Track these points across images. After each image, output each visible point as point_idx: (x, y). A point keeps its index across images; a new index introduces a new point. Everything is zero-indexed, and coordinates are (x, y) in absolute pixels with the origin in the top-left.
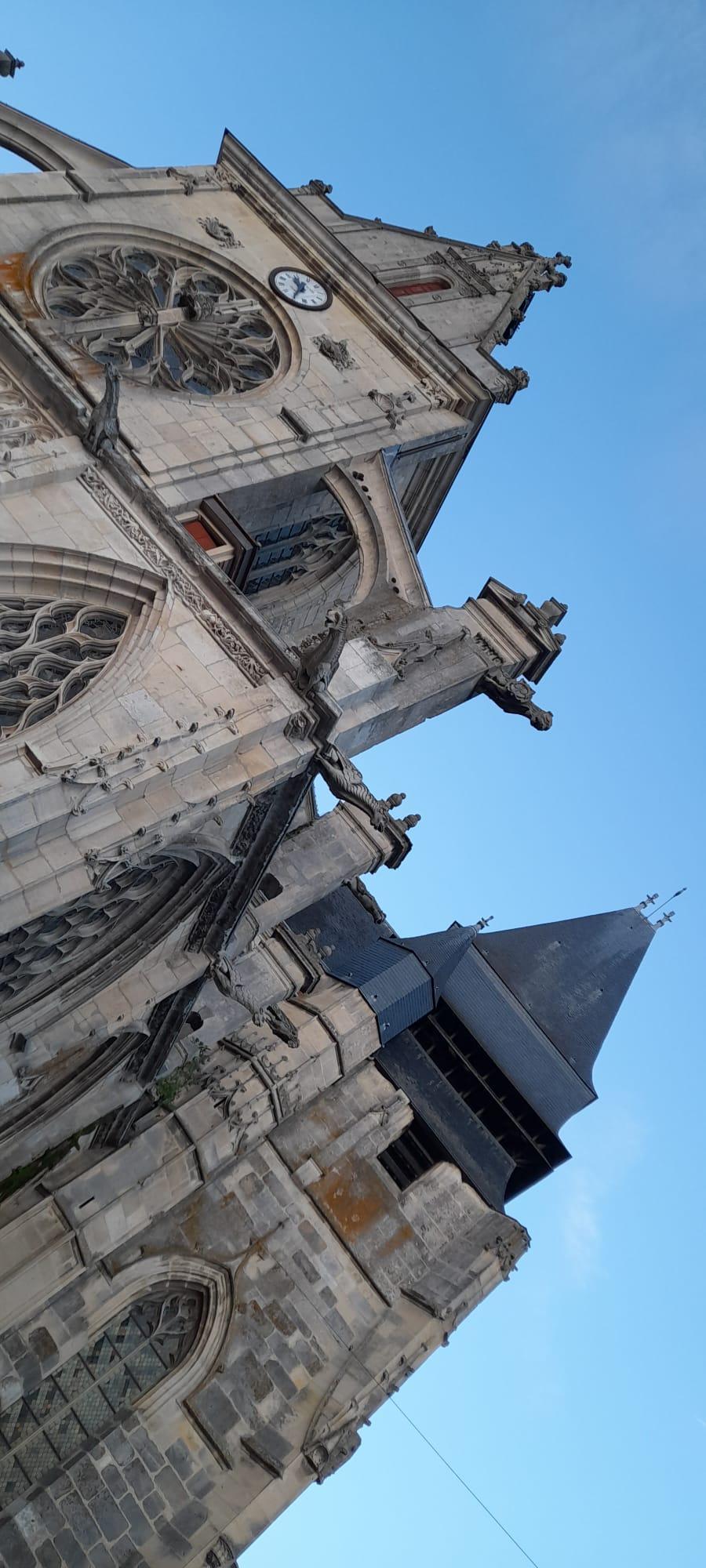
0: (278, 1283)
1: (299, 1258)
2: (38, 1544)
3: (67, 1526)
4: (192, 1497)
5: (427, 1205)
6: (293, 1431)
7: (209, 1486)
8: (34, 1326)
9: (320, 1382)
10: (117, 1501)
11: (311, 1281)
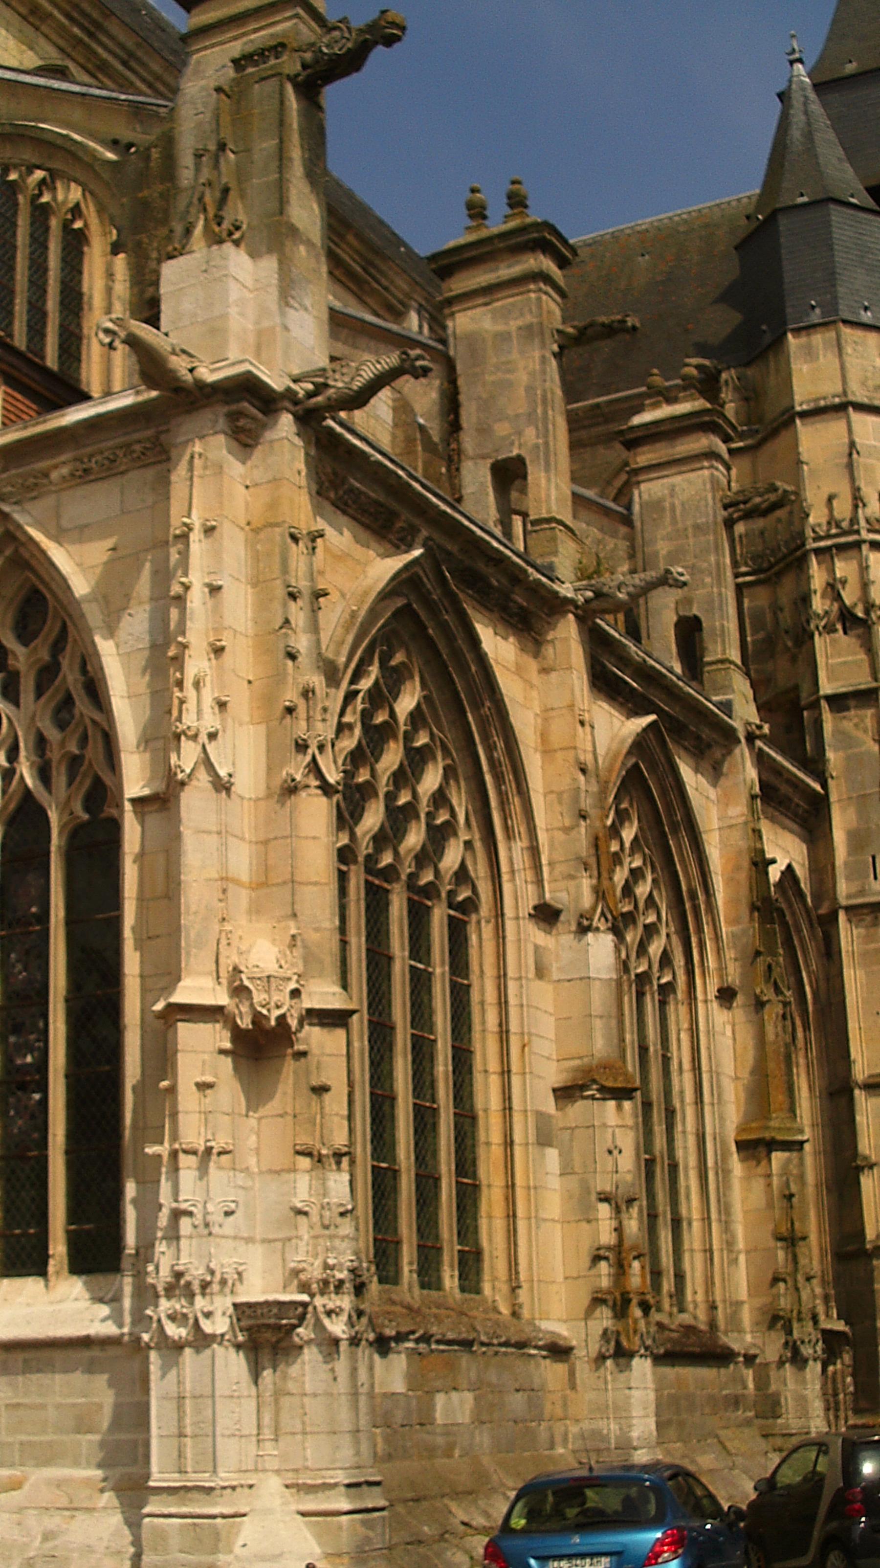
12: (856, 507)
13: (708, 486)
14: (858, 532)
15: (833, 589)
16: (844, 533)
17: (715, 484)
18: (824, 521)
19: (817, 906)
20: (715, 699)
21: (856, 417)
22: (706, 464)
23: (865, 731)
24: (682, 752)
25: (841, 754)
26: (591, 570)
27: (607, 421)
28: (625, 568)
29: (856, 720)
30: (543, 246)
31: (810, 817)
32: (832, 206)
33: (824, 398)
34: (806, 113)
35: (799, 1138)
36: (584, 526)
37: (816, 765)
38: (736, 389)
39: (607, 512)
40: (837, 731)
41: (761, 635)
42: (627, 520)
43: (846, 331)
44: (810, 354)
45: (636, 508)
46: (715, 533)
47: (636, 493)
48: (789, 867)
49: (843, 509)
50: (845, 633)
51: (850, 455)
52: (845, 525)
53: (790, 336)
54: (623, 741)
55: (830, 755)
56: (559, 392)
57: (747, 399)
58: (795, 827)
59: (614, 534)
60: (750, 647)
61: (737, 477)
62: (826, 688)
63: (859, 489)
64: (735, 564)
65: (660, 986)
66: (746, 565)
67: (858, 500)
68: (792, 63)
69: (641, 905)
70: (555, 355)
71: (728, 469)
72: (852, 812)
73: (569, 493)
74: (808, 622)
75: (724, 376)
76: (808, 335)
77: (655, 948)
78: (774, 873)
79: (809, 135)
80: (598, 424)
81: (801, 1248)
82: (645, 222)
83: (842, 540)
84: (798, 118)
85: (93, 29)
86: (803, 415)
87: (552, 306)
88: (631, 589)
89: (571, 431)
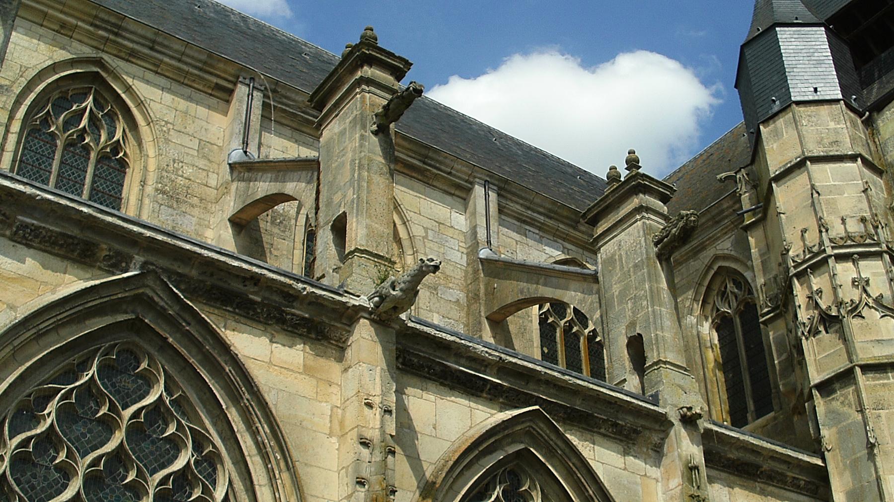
12: (821, 232)
16: (816, 255)
23: (850, 406)
25: (834, 430)
29: (842, 398)
40: (830, 412)
49: (812, 238)
50: (827, 332)
55: (824, 432)
67: (822, 227)
72: (847, 475)
76: (774, 122)
85: (116, 30)
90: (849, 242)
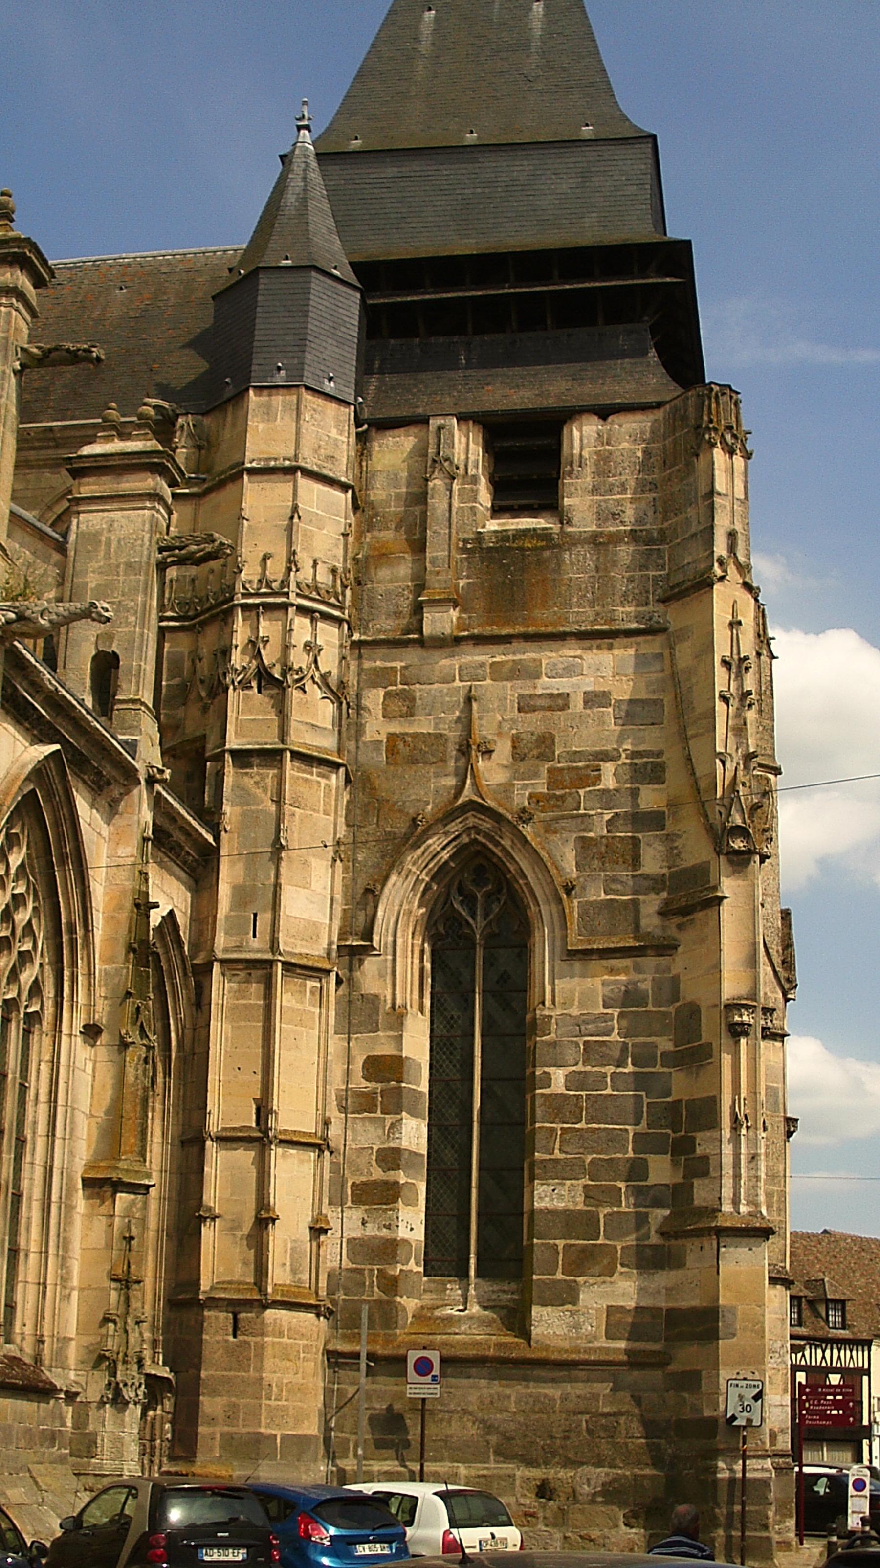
0: (533, 750)
1: (525, 706)
2: (580, 1199)
3: (589, 1158)
4: (671, 1009)
5: (595, 490)
6: (696, 850)
7: (675, 981)
8: (358, 1066)
9: (676, 778)
10: (609, 1091)
11: (565, 707)
12: (289, 570)
13: (147, 526)
14: (287, 594)
15: (254, 646)
17: (154, 526)
18: (255, 579)
19: (193, 956)
20: (120, 737)
21: (302, 481)
22: (148, 504)
23: (265, 790)
24: (81, 785)
25: (238, 809)
26: (18, 592)
27: (57, 447)
28: (52, 595)
29: (257, 778)
30: (22, 263)
31: (200, 867)
32: (313, 274)
33: (276, 459)
34: (304, 179)
35: (146, 1182)
36: (17, 546)
37: (211, 817)
38: (190, 435)
39: (42, 536)
40: (237, 787)
41: (177, 681)
42: (61, 548)
43: (307, 397)
44: (268, 413)
45: (72, 537)
46: (147, 574)
47: (75, 522)
48: (171, 912)
49: (276, 570)
50: (259, 692)
51: (292, 518)
52: (275, 585)
53: (251, 392)
54: (23, 767)
55: (227, 808)
56: (13, 410)
57: (199, 448)
58: (183, 875)
59: (46, 560)
60: (164, 691)
61: (179, 522)
62: (233, 742)
63: (294, 553)
64: (162, 607)
65: (27, 1014)
66: (173, 610)
67: (292, 563)
68: (299, 128)
69: (19, 932)
70: (15, 372)
71: (170, 513)
73: (8, 511)
74: (225, 674)
75: (181, 420)
77: (27, 977)
78: (156, 918)
79: (303, 201)
80: (48, 448)
81: (135, 1292)
82: (128, 256)
83: (270, 600)
84: (296, 183)
86: (252, 472)
87: (21, 323)
88: (54, 617)
89: (19, 450)
90: (314, 595)
